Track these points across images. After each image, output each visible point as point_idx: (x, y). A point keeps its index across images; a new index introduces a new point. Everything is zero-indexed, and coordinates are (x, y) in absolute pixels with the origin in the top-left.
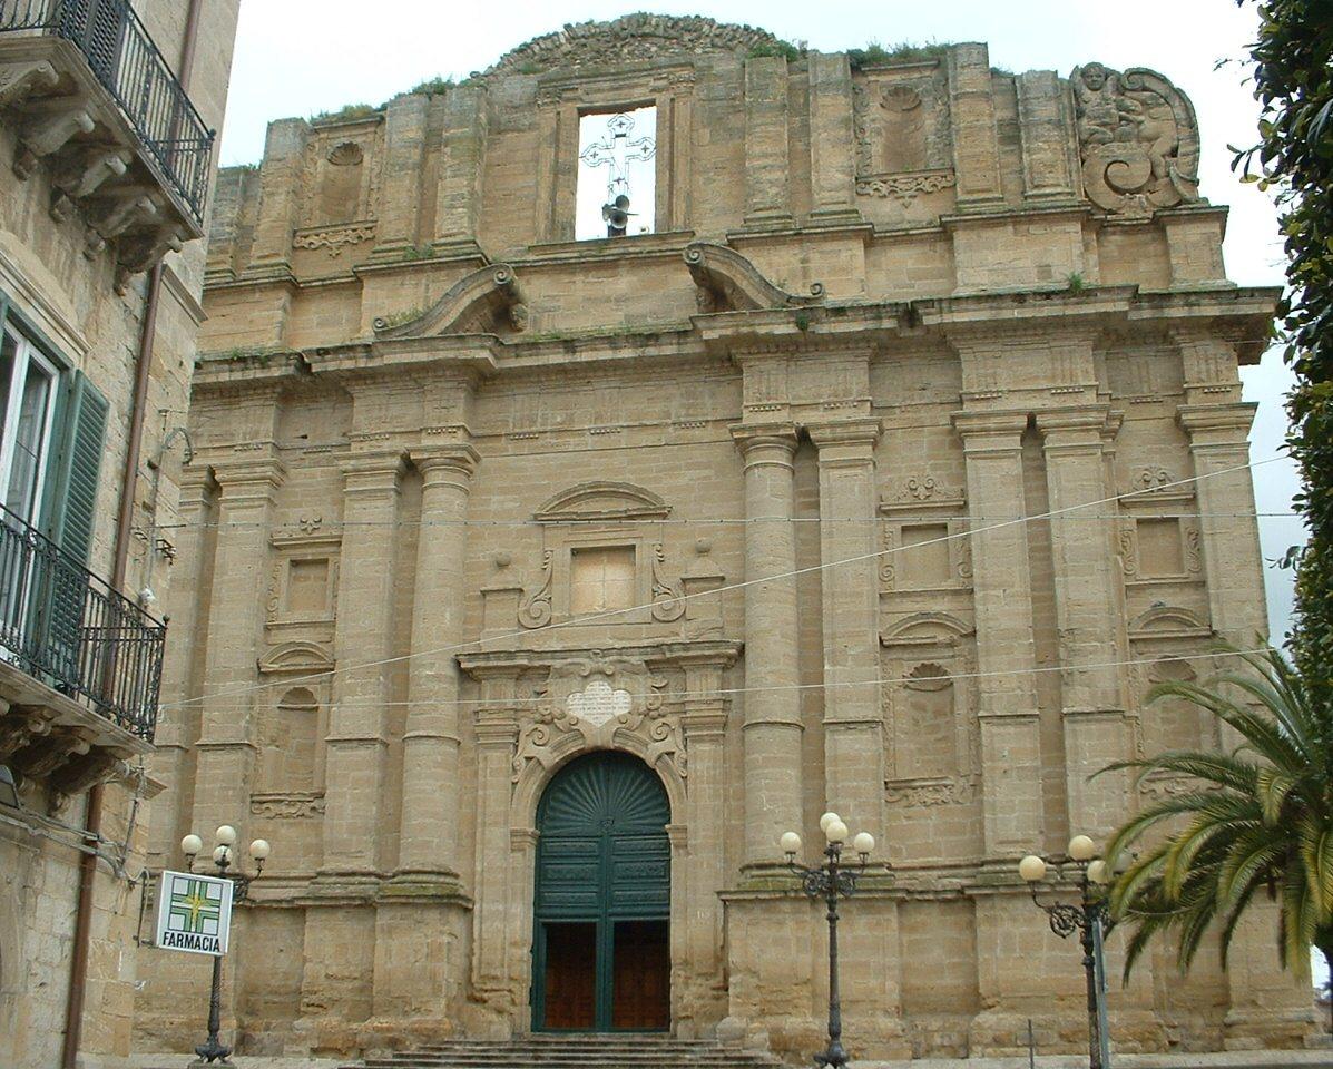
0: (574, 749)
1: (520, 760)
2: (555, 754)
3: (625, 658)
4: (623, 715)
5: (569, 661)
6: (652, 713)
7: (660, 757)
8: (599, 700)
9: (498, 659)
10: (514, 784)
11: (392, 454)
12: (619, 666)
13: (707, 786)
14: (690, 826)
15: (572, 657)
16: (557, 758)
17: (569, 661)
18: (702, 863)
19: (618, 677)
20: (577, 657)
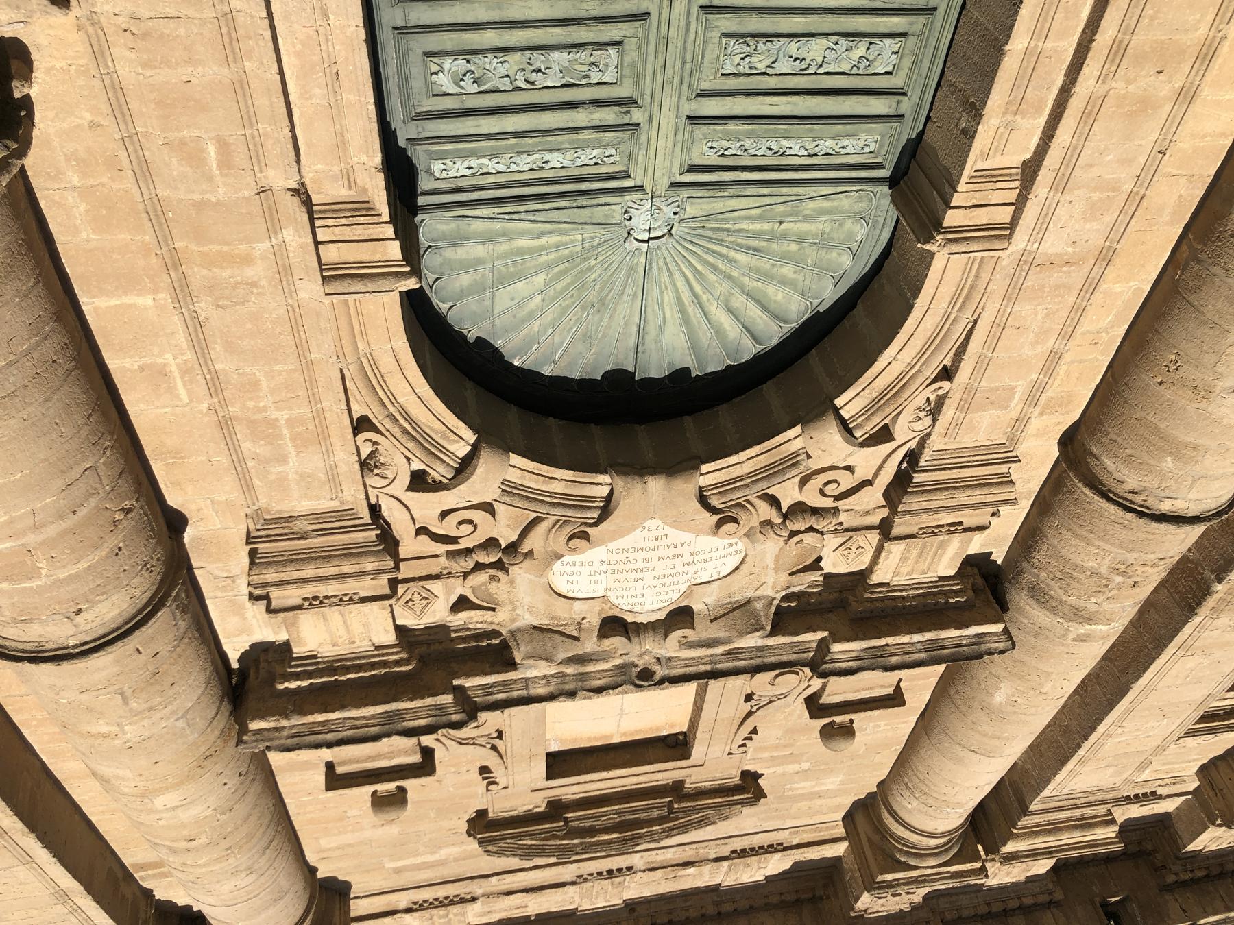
0: (733, 459)
1: (905, 433)
2: (797, 445)
3: (570, 670)
4: (574, 550)
5: (720, 650)
6: (493, 558)
7: (465, 467)
8: (648, 577)
9: (906, 650)
10: (947, 374)
11: (1012, 857)
12: (590, 645)
13: (274, 414)
14: (310, 289)
15: (712, 660)
16: (792, 439)
17: (720, 650)
18: (226, 162)
19: (595, 621)
20: (692, 662)
